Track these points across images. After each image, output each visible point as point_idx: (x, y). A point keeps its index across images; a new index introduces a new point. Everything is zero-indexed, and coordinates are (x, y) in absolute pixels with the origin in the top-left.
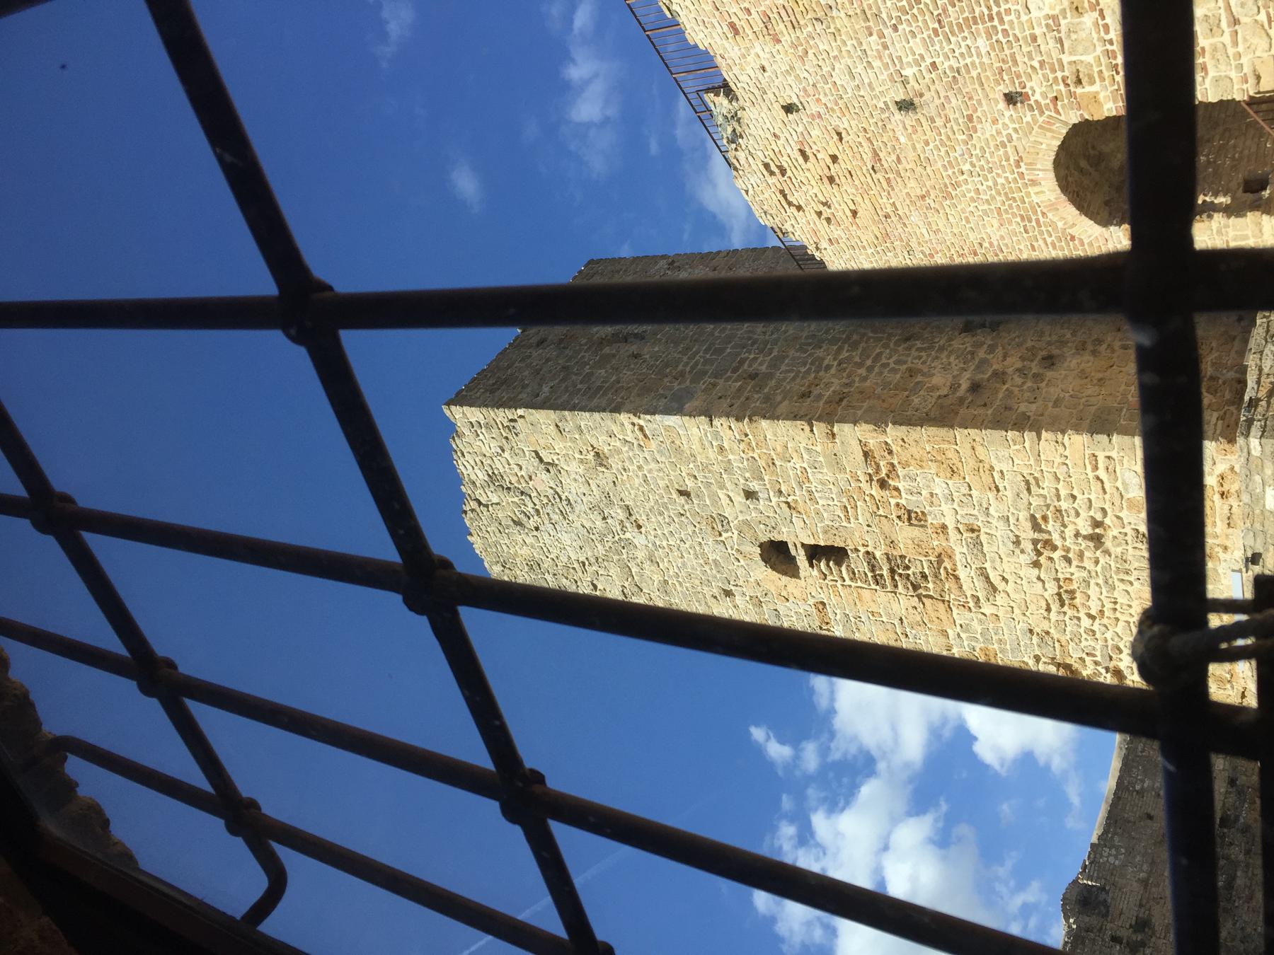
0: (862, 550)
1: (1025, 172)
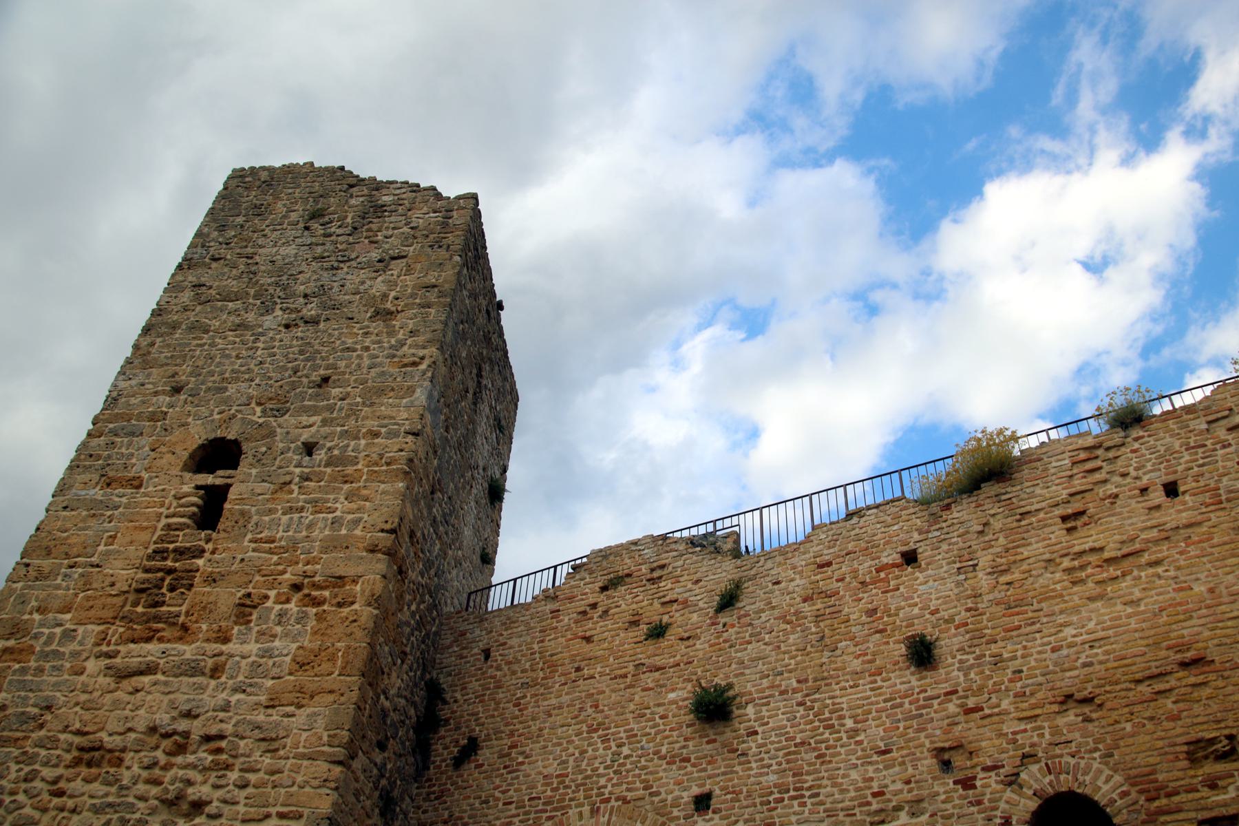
0: (210, 546)
1: (609, 805)
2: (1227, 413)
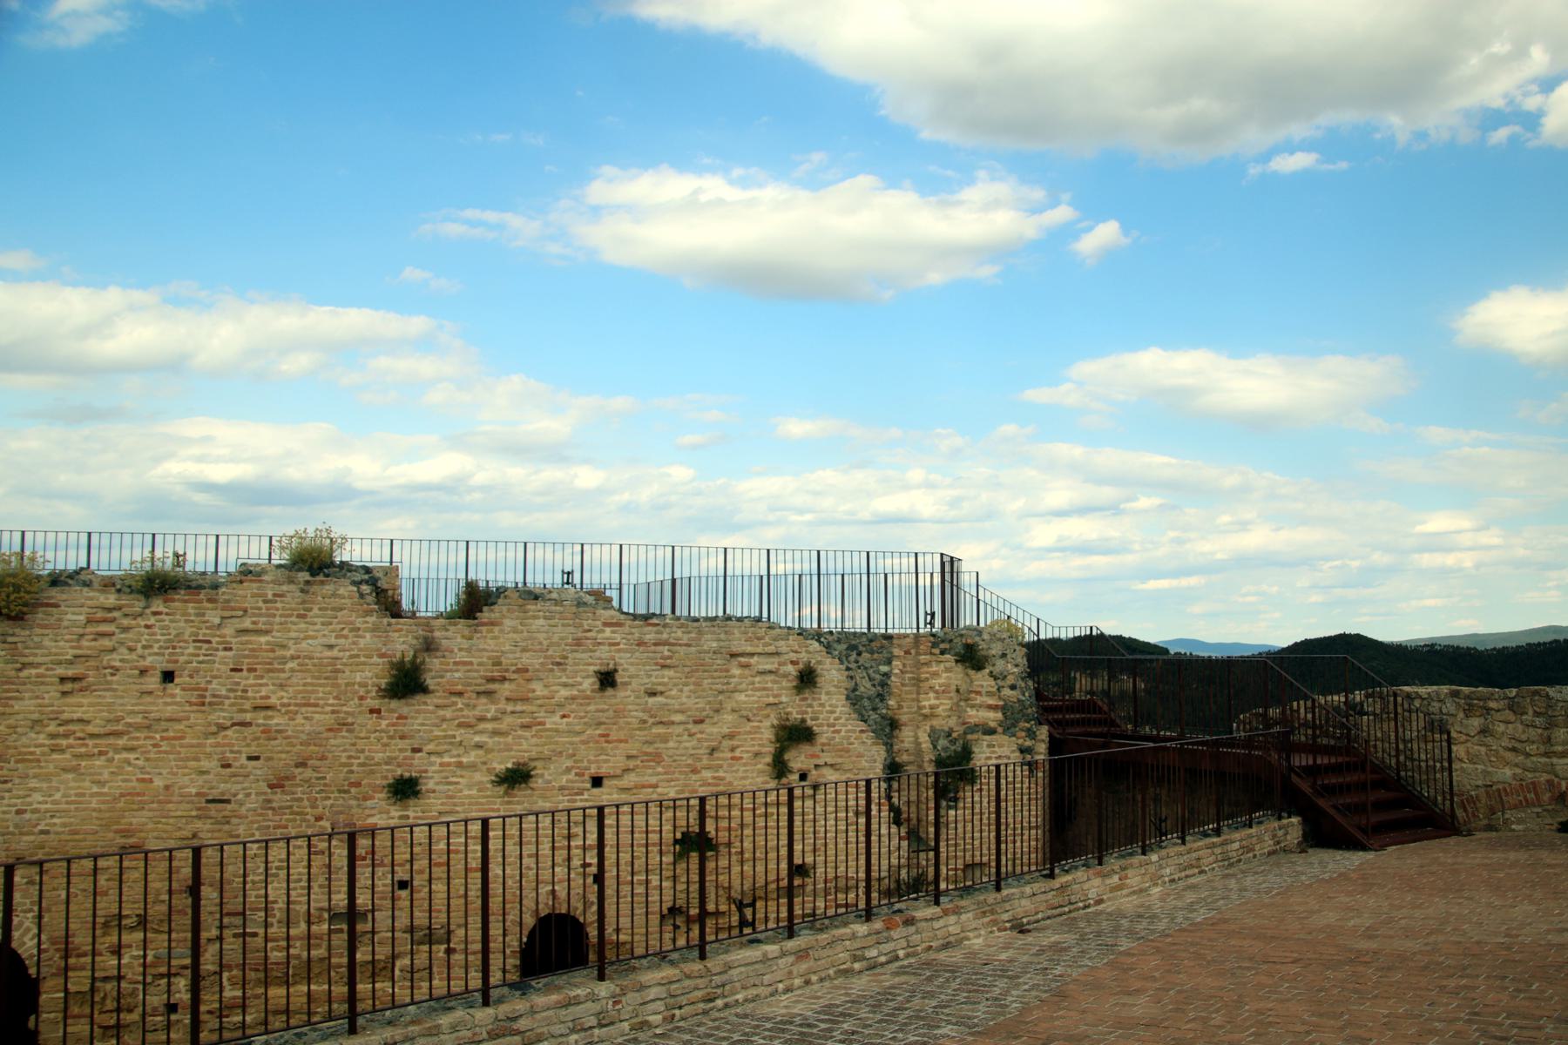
2: (241, 613)
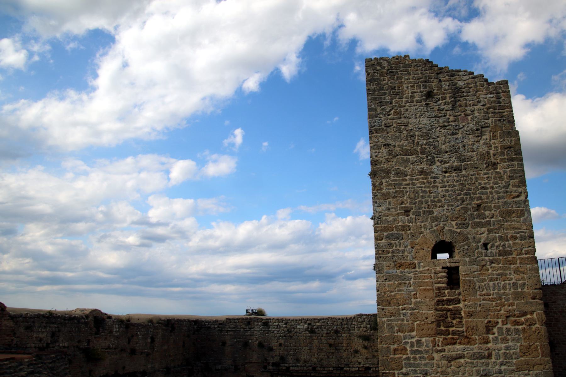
0: (460, 297)
